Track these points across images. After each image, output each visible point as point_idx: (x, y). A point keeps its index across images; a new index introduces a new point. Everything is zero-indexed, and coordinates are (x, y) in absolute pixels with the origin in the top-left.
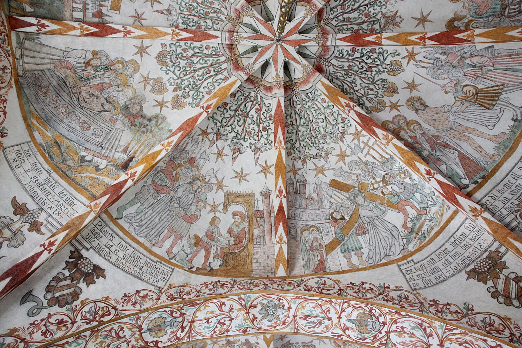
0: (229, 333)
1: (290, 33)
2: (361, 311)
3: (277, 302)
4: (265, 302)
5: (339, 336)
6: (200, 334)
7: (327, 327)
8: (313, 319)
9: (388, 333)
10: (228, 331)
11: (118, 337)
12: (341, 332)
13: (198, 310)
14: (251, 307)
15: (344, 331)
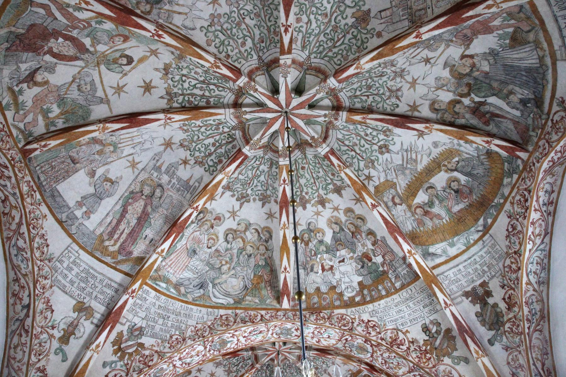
0: (315, 326)
1: (272, 354)
2: (225, 349)
3: (281, 336)
4: (289, 337)
5: (236, 331)
6: (336, 332)
7: (245, 332)
8: (256, 333)
9: (205, 348)
10: (316, 328)
11: (386, 362)
12: (235, 333)
13: (334, 345)
14: (299, 337)
15: (233, 335)
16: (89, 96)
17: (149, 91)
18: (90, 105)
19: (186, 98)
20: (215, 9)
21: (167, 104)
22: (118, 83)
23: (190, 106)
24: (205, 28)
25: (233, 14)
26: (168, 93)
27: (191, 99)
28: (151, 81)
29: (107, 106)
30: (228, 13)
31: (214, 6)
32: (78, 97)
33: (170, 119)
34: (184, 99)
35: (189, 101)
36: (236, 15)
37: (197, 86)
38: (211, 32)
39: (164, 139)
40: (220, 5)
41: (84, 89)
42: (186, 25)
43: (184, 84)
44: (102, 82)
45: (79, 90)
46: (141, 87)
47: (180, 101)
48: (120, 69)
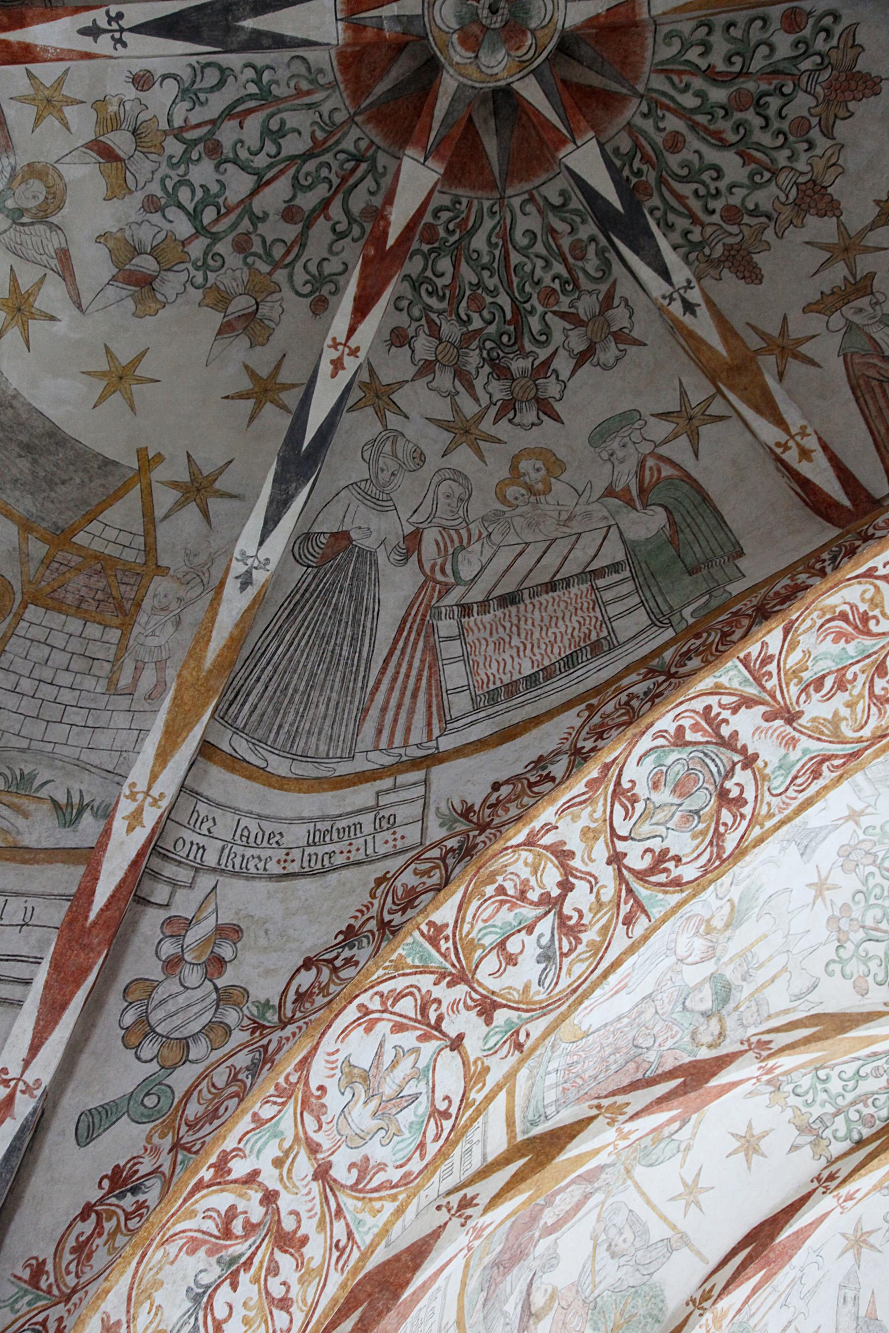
16: (640, 1253)
17: (756, 1151)
18: (651, 1274)
19: (854, 1116)
20: (828, 903)
21: (817, 1156)
22: (682, 1179)
23: (874, 1130)
24: (834, 961)
25: (871, 882)
26: (803, 1129)
27: (866, 1111)
28: (750, 1127)
29: (686, 1250)
30: (860, 887)
31: (824, 900)
32: (619, 1274)
33: (850, 1198)
34: (848, 1120)
35: (864, 1120)
36: (878, 879)
37: (862, 1073)
38: (851, 958)
39: (843, 1235)
40: (835, 887)
41: (622, 1246)
42: (796, 991)
43: (828, 1086)
44: (649, 1202)
45: (613, 1255)
46: (735, 1152)
47: (841, 1133)
48: (673, 1146)
